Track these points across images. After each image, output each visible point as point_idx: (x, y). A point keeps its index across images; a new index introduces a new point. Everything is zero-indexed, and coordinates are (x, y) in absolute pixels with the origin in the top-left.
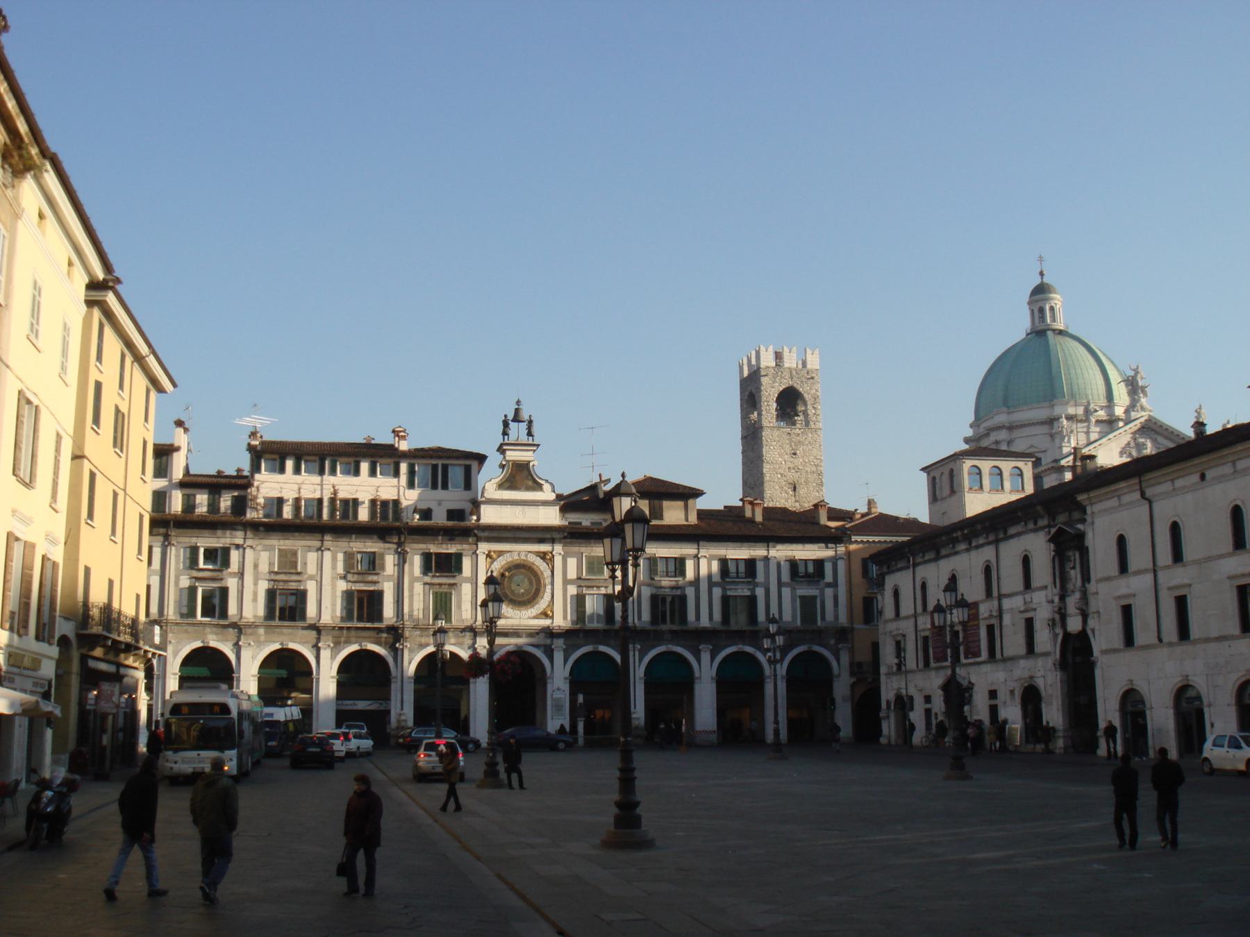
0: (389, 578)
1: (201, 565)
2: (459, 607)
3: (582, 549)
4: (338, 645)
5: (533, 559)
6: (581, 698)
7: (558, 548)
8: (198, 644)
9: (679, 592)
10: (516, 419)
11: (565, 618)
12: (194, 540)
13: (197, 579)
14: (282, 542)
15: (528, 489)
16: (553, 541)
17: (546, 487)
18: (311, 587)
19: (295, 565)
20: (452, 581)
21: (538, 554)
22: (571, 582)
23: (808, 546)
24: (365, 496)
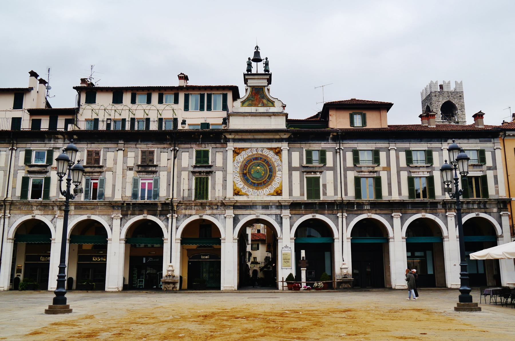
0: (165, 168)
1: (33, 162)
2: (214, 188)
3: (303, 145)
4: (125, 216)
5: (266, 153)
6: (303, 253)
7: (284, 146)
8: (29, 217)
9: (375, 175)
10: (257, 59)
11: (291, 194)
12: (28, 146)
13: (29, 172)
14: (89, 145)
15: (264, 105)
16: (281, 140)
17: (276, 104)
18: (108, 176)
19: (97, 161)
20: (208, 170)
21: (271, 149)
22: (296, 169)
23: (471, 141)
24: (154, 117)
